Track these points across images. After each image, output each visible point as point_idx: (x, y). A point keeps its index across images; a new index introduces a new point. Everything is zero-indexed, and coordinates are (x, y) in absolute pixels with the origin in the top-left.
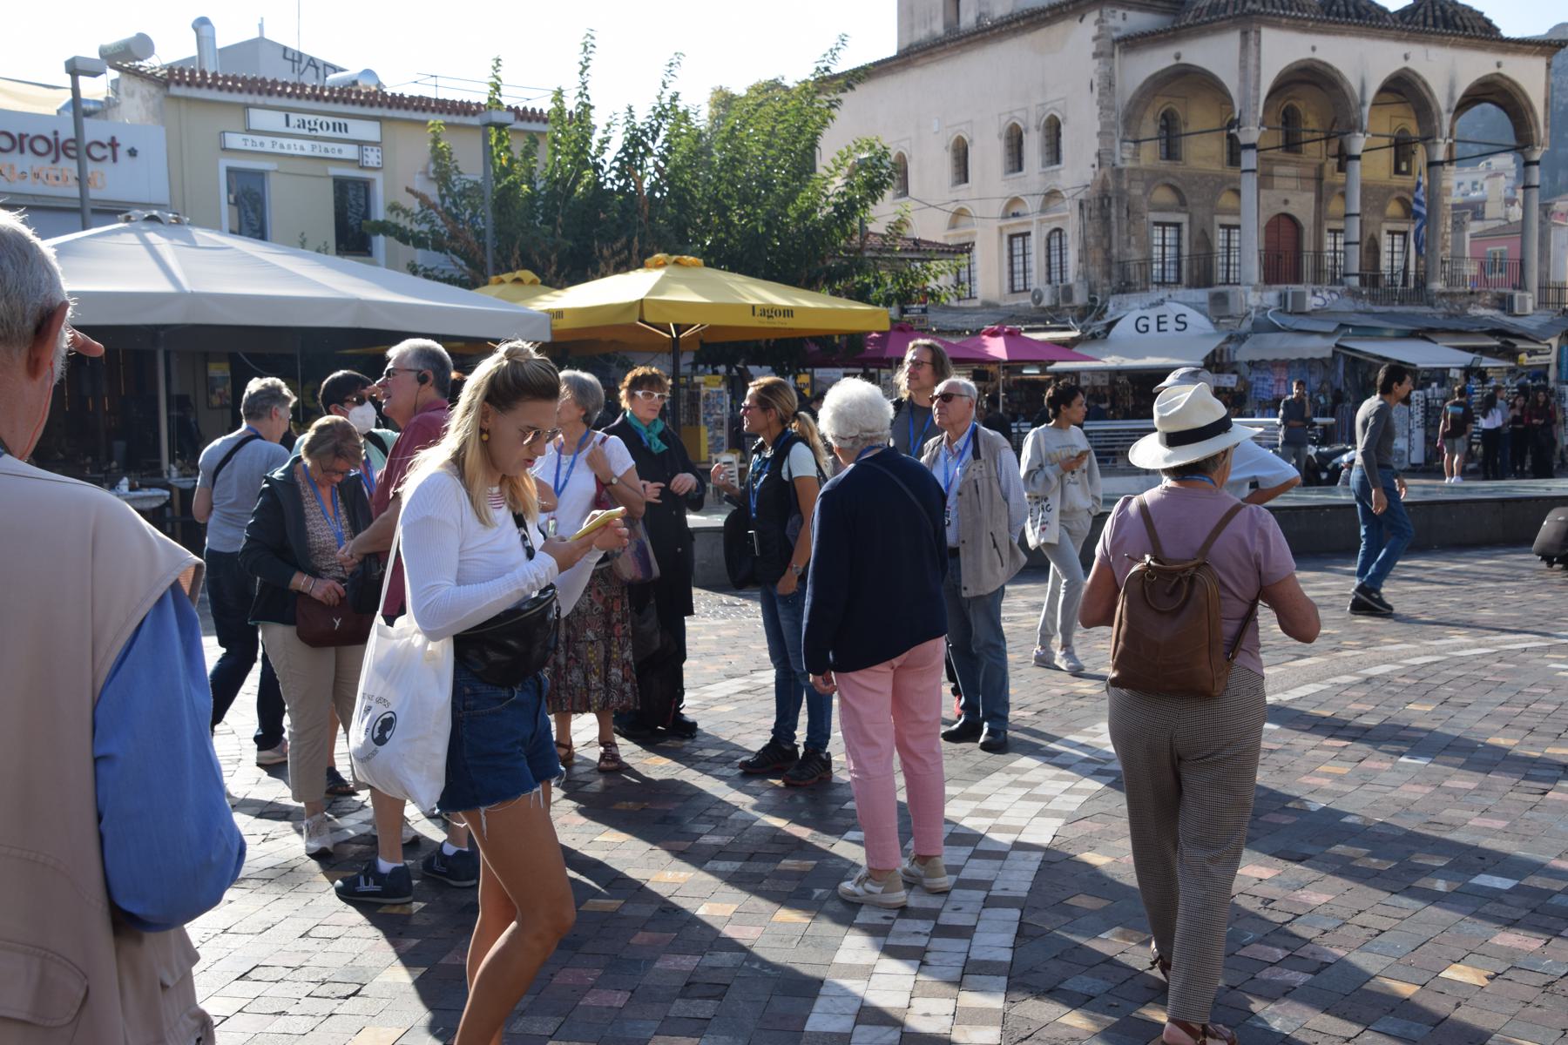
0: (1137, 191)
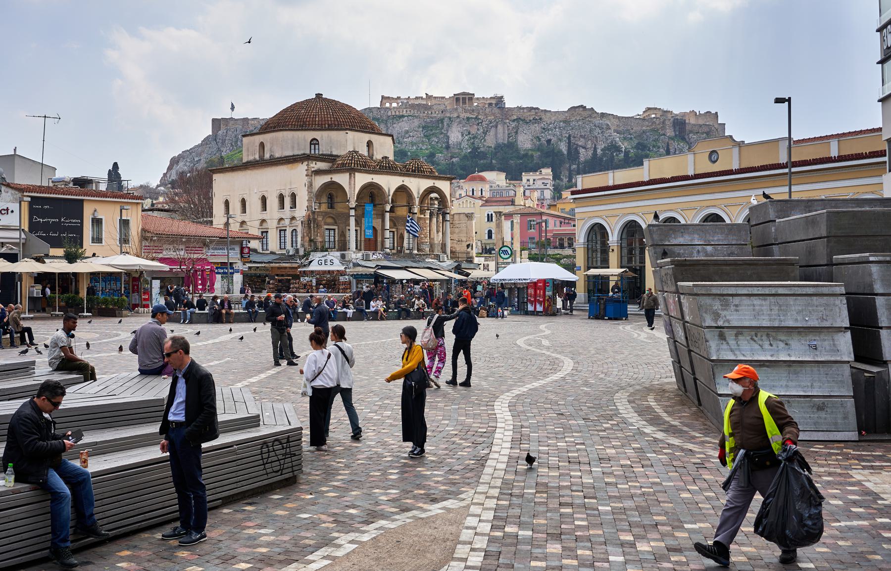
0: (320, 219)
